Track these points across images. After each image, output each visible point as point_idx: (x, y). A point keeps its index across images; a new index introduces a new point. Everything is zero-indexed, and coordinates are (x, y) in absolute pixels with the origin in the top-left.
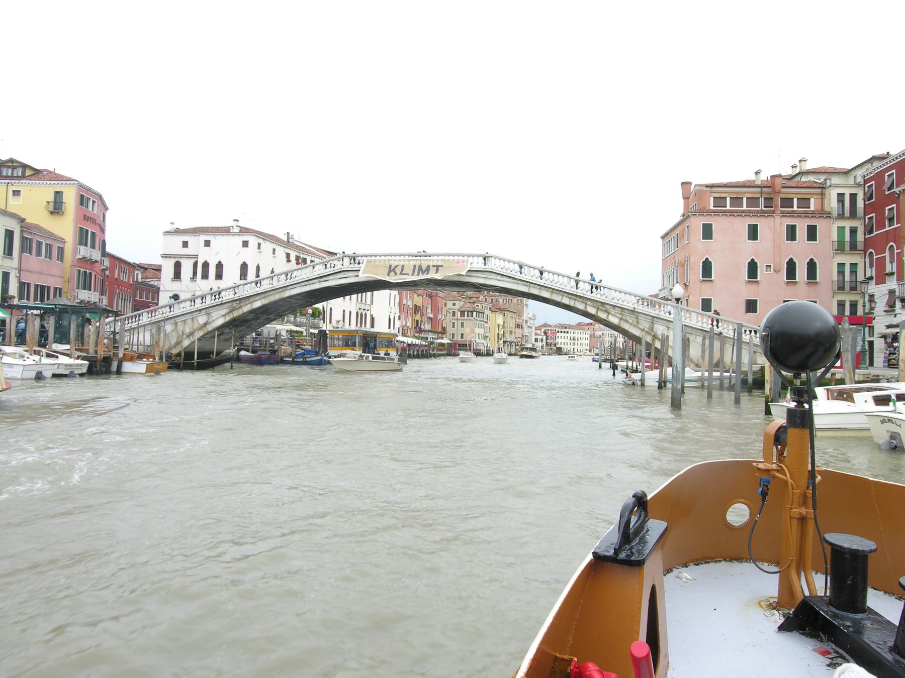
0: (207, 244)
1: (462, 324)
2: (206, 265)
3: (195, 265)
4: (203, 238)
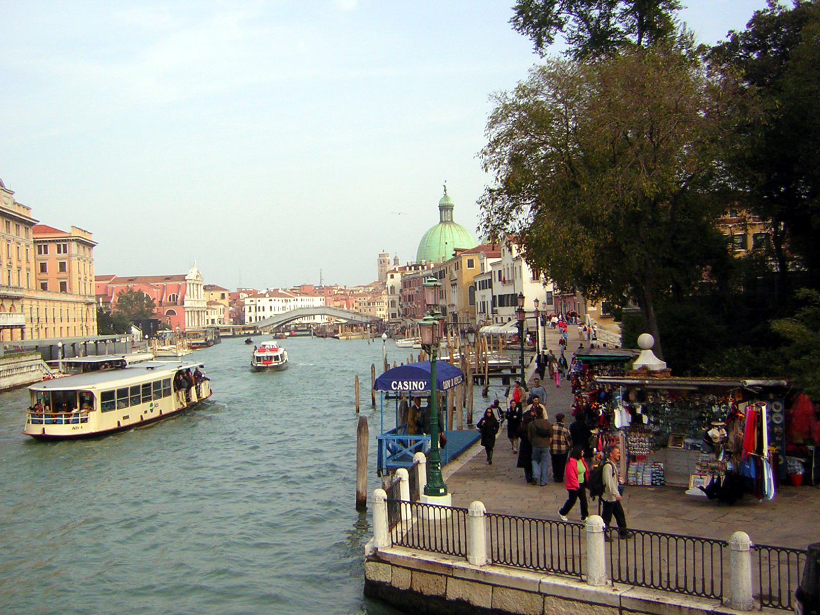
0: (259, 301)
1: (370, 310)
2: (259, 308)
3: (256, 307)
4: (258, 299)
